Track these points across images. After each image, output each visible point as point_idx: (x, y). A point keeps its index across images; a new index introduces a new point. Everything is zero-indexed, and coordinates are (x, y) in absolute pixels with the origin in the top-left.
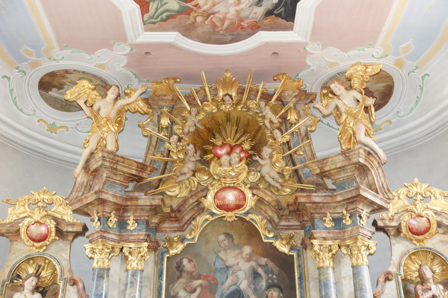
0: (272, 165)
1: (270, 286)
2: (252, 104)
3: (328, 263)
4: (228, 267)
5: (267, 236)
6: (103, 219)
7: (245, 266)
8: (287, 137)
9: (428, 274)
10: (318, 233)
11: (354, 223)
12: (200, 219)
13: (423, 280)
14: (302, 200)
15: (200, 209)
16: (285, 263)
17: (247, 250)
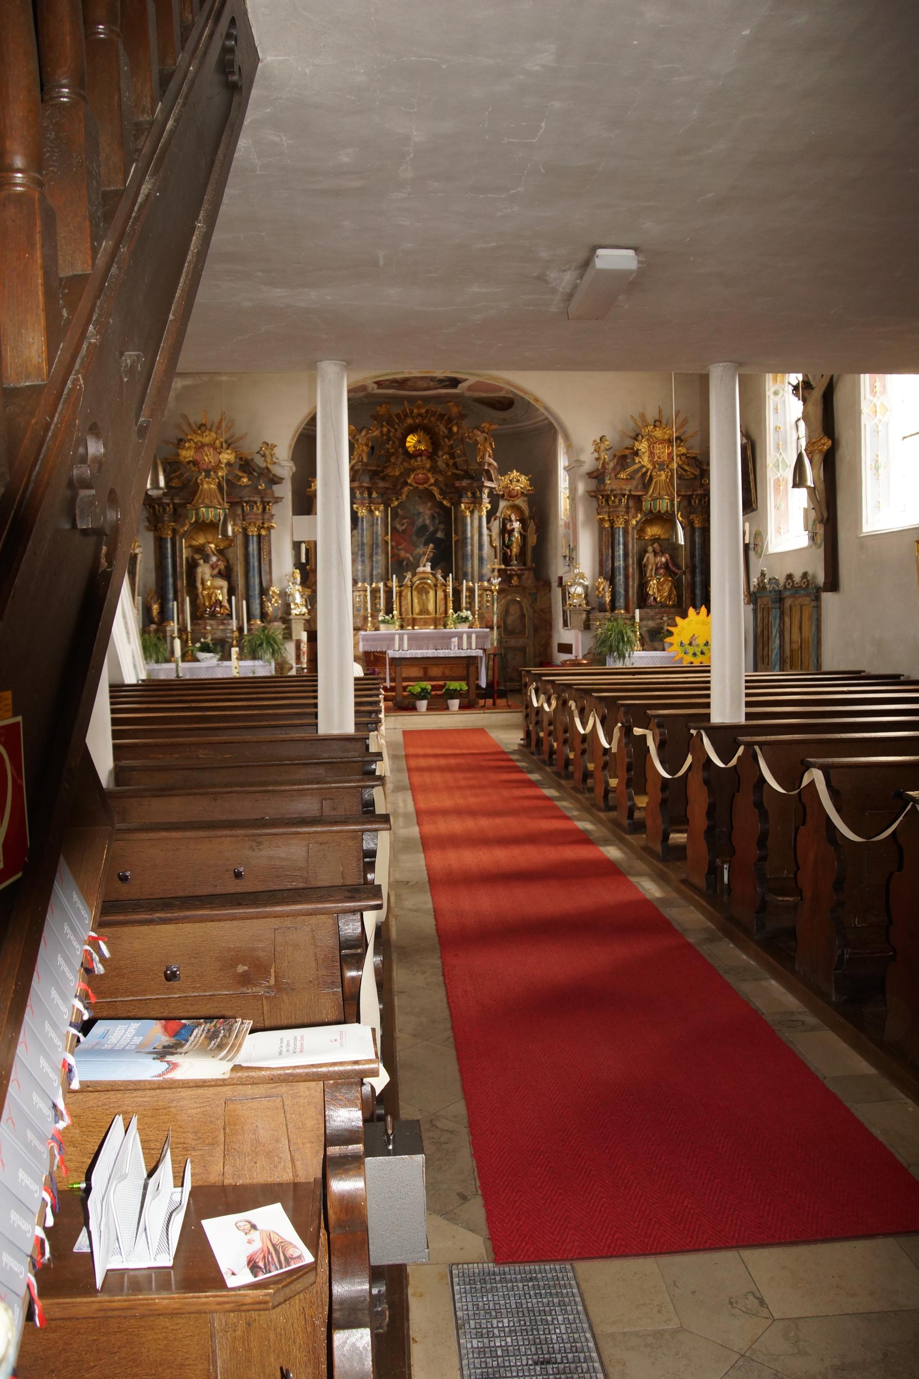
0: (443, 459)
1: (439, 523)
2: (433, 419)
3: (468, 514)
4: (420, 513)
5: (438, 497)
7: (428, 512)
8: (452, 442)
9: (513, 517)
10: (464, 500)
11: (481, 497)
12: (406, 489)
13: (511, 521)
14: (457, 485)
15: (406, 483)
16: (447, 511)
17: (429, 504)
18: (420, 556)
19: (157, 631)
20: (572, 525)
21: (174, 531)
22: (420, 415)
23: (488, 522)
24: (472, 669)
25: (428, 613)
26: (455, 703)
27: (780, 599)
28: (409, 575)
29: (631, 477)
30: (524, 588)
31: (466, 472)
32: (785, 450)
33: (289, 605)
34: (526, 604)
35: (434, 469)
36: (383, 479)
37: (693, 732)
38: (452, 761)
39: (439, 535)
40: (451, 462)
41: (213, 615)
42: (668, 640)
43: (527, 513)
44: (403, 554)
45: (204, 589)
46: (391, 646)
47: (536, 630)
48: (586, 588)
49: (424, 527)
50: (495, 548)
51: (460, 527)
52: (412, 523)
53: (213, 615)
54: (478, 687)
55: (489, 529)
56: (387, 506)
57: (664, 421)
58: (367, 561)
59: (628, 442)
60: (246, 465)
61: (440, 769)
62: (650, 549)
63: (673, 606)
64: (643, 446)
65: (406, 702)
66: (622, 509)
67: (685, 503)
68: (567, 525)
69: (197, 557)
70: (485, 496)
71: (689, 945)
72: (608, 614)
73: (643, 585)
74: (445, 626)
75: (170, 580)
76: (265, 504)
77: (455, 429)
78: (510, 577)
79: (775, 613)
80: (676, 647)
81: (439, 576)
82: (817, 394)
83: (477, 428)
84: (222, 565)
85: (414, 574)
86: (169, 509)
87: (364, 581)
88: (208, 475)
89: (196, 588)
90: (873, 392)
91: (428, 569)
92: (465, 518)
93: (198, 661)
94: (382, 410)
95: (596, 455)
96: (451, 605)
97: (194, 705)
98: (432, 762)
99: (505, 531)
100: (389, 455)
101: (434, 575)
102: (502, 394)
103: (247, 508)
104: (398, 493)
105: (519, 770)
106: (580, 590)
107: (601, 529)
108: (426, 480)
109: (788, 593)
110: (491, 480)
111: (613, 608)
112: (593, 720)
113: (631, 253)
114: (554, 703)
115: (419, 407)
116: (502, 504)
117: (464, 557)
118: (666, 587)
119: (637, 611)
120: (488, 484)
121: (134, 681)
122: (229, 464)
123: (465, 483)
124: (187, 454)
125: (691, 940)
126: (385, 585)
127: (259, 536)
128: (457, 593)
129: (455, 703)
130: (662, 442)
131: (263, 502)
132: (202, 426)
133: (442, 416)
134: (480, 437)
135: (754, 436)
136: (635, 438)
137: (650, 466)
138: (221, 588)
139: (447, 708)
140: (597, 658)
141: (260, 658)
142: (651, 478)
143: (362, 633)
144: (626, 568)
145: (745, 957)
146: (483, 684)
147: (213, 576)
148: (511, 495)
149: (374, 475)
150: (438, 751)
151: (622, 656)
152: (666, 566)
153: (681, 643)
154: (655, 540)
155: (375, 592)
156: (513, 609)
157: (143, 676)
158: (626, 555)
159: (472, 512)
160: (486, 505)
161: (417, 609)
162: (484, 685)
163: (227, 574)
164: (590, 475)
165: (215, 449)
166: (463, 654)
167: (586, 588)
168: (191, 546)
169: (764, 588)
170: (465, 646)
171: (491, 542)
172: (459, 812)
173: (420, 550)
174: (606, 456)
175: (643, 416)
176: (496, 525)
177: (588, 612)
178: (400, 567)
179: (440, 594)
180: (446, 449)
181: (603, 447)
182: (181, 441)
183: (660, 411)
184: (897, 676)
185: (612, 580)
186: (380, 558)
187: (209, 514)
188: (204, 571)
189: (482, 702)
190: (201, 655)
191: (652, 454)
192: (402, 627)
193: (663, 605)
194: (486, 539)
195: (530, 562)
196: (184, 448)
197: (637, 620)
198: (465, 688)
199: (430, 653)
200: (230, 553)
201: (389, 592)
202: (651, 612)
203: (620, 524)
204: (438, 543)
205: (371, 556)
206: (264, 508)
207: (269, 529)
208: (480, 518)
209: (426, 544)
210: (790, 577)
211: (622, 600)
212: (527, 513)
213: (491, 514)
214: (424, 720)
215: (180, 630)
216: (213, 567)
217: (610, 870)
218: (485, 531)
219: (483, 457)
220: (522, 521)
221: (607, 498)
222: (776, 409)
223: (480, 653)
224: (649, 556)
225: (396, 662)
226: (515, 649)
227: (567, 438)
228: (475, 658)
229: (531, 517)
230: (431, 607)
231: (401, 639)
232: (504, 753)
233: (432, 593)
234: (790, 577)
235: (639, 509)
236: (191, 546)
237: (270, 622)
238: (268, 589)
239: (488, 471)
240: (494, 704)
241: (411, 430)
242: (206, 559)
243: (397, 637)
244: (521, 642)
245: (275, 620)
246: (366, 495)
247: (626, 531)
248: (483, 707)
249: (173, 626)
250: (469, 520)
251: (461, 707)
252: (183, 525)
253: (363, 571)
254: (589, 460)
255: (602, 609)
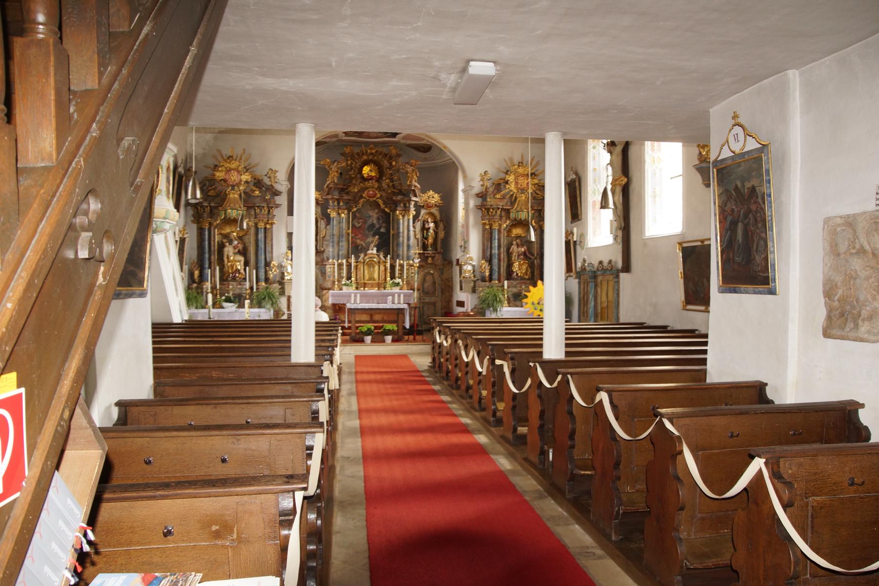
0: (385, 182)
2: (380, 157)
3: (401, 217)
5: (382, 206)
6: (333, 202)
7: (375, 216)
9: (430, 220)
10: (399, 208)
12: (361, 201)
15: (361, 197)
16: (388, 215)
18: (370, 243)
19: (197, 288)
20: (466, 226)
21: (210, 224)
22: (372, 154)
23: (414, 222)
24: (400, 316)
25: (374, 280)
26: (389, 338)
27: (594, 276)
28: (362, 255)
29: (503, 197)
30: (436, 265)
31: (400, 190)
32: (599, 183)
33: (283, 273)
34: (436, 276)
35: (380, 189)
36: (347, 193)
37: (532, 364)
38: (385, 376)
39: (382, 230)
40: (391, 184)
41: (234, 279)
42: (524, 300)
43: (438, 218)
44: (358, 241)
45: (228, 262)
46: (349, 301)
47: (442, 292)
48: (474, 266)
49: (373, 225)
50: (418, 239)
51: (396, 226)
52: (365, 222)
53: (234, 279)
54: (404, 328)
55: (414, 227)
56: (349, 211)
57: (525, 163)
58: (336, 245)
59: (502, 175)
60: (258, 183)
61: (377, 382)
62: (514, 243)
63: (528, 279)
64: (511, 178)
65: (358, 337)
66: (497, 217)
67: (537, 214)
68: (463, 226)
69: (225, 241)
70: (412, 206)
71: (525, 501)
72: (487, 284)
73: (510, 265)
74: (385, 288)
75: (207, 255)
76: (269, 208)
77: (394, 163)
78: (427, 258)
79: (592, 285)
80: (530, 305)
81: (382, 256)
82: (619, 149)
83: (407, 163)
84: (240, 247)
85: (366, 255)
86: (208, 210)
87: (333, 259)
88: (233, 189)
89: (223, 261)
90: (653, 150)
91: (375, 251)
92: (398, 220)
93: (222, 307)
94: (347, 150)
95: (481, 183)
96: (388, 274)
97: (215, 339)
98: (372, 377)
99: (424, 229)
100: (351, 179)
101: (378, 256)
102: (424, 142)
103: (258, 211)
104: (356, 203)
105: (426, 383)
106: (470, 268)
107: (484, 230)
108: (375, 195)
109: (599, 273)
110: (416, 196)
111: (491, 279)
112: (473, 353)
113: (492, 64)
114: (449, 341)
115: (371, 149)
116: (423, 212)
117: (398, 245)
118: (524, 267)
119: (506, 282)
120: (414, 199)
121: (180, 321)
122: (247, 182)
123: (399, 197)
124: (220, 175)
125: (527, 498)
126: (347, 261)
127: (265, 228)
128: (393, 267)
129: (389, 338)
130: (523, 175)
131: (268, 207)
132: (230, 157)
133: (386, 155)
134: (410, 169)
135: (580, 174)
136: (507, 173)
137: (515, 191)
138: (240, 261)
139: (384, 341)
140: (480, 311)
141: (264, 307)
142: (516, 198)
143: (331, 291)
144: (499, 254)
145: (560, 509)
146: (408, 326)
147: (235, 254)
148: (428, 206)
149: (342, 191)
150: (376, 370)
151: (495, 310)
152: (524, 254)
153: (533, 303)
154: (518, 237)
155: (340, 265)
156: (429, 278)
157: (186, 318)
158: (499, 246)
159: (403, 216)
160: (413, 212)
161: (367, 277)
162: (408, 326)
163: (244, 252)
164: (478, 195)
165: (238, 172)
166: (395, 306)
167: (474, 266)
168: (221, 234)
169: (585, 269)
170: (396, 302)
171: (415, 235)
172: (386, 411)
173: (370, 239)
174: (488, 184)
175: (511, 159)
176: (419, 225)
177: (475, 282)
178: (357, 250)
179: (382, 268)
180: (388, 176)
181: (486, 178)
182: (216, 166)
183: (522, 157)
184: (666, 327)
185: (490, 262)
186: (344, 244)
187: (233, 214)
188: (229, 250)
189: (406, 337)
190: (225, 304)
191: (517, 183)
192: (357, 288)
193: (522, 278)
194: (412, 233)
195: (439, 250)
196: (218, 171)
197: (506, 287)
198: (396, 328)
199: (374, 306)
200: (246, 239)
201: (349, 266)
202: (514, 283)
203: (496, 227)
204: (381, 235)
205: (339, 242)
206: (269, 211)
207: (272, 224)
208: (409, 220)
209: (374, 235)
210: (601, 262)
211: (496, 274)
212: (438, 218)
213: (416, 218)
214: (368, 348)
215: (212, 288)
216: (235, 248)
217: (480, 451)
218: (411, 228)
219: (411, 182)
220: (435, 222)
221: (488, 210)
222: (594, 157)
223: (406, 306)
224: (514, 248)
225: (352, 311)
226: (429, 303)
227: (464, 172)
228: (403, 309)
229: (441, 220)
230: (376, 276)
231: (356, 296)
232: (418, 371)
233: (377, 267)
234: (601, 262)
235: (508, 217)
236: (221, 234)
237: (271, 284)
238: (270, 263)
239: (414, 191)
240: (414, 339)
241: (366, 163)
242: (231, 242)
243: (353, 295)
244: (433, 299)
245: (274, 283)
246: (336, 203)
247: (499, 231)
248: (407, 341)
249: (208, 285)
250: (401, 221)
251: (393, 341)
252: (216, 220)
253: (333, 252)
254: (477, 187)
255: (483, 280)
